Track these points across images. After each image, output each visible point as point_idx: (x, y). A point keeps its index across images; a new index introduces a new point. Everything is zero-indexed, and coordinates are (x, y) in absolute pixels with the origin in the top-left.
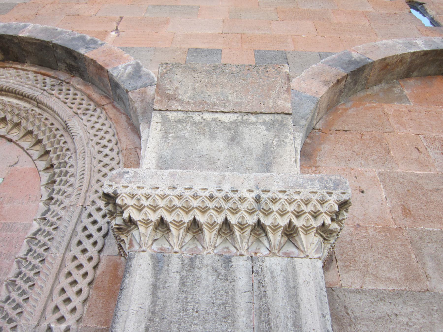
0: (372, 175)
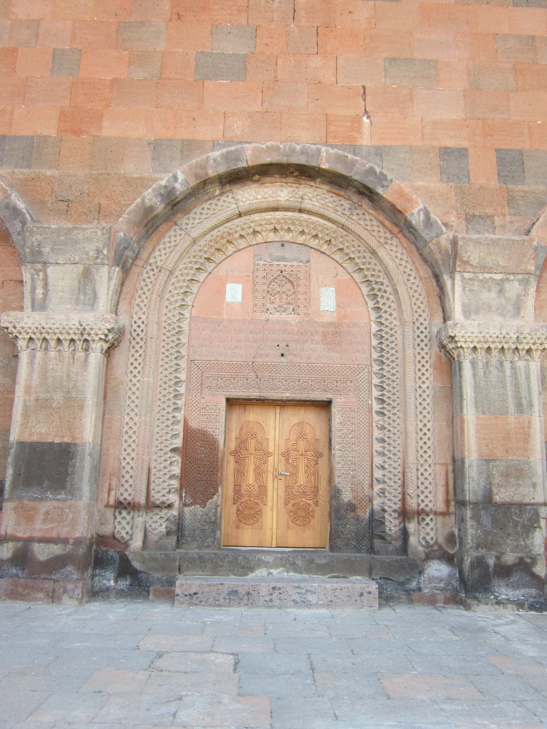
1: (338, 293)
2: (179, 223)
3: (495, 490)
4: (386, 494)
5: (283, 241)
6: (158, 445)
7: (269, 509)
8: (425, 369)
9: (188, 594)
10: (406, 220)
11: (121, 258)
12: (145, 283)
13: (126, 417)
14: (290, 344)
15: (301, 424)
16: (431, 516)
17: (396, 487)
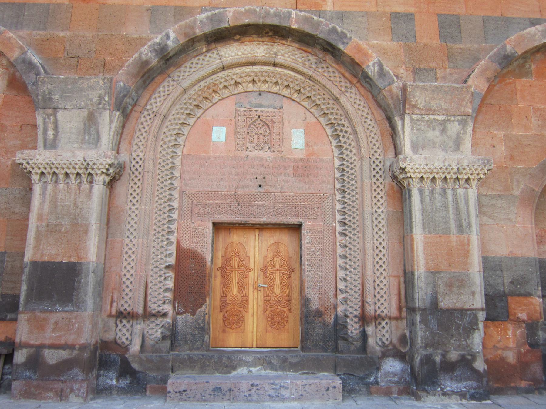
0: (500, 136)
1: (306, 134)
2: (171, 75)
3: (440, 298)
4: (348, 302)
5: (260, 91)
6: (154, 263)
7: (250, 315)
8: (380, 196)
9: (178, 391)
10: (363, 71)
11: (121, 104)
12: (143, 126)
13: (126, 240)
14: (266, 177)
15: (276, 243)
16: (387, 320)
17: (357, 296)
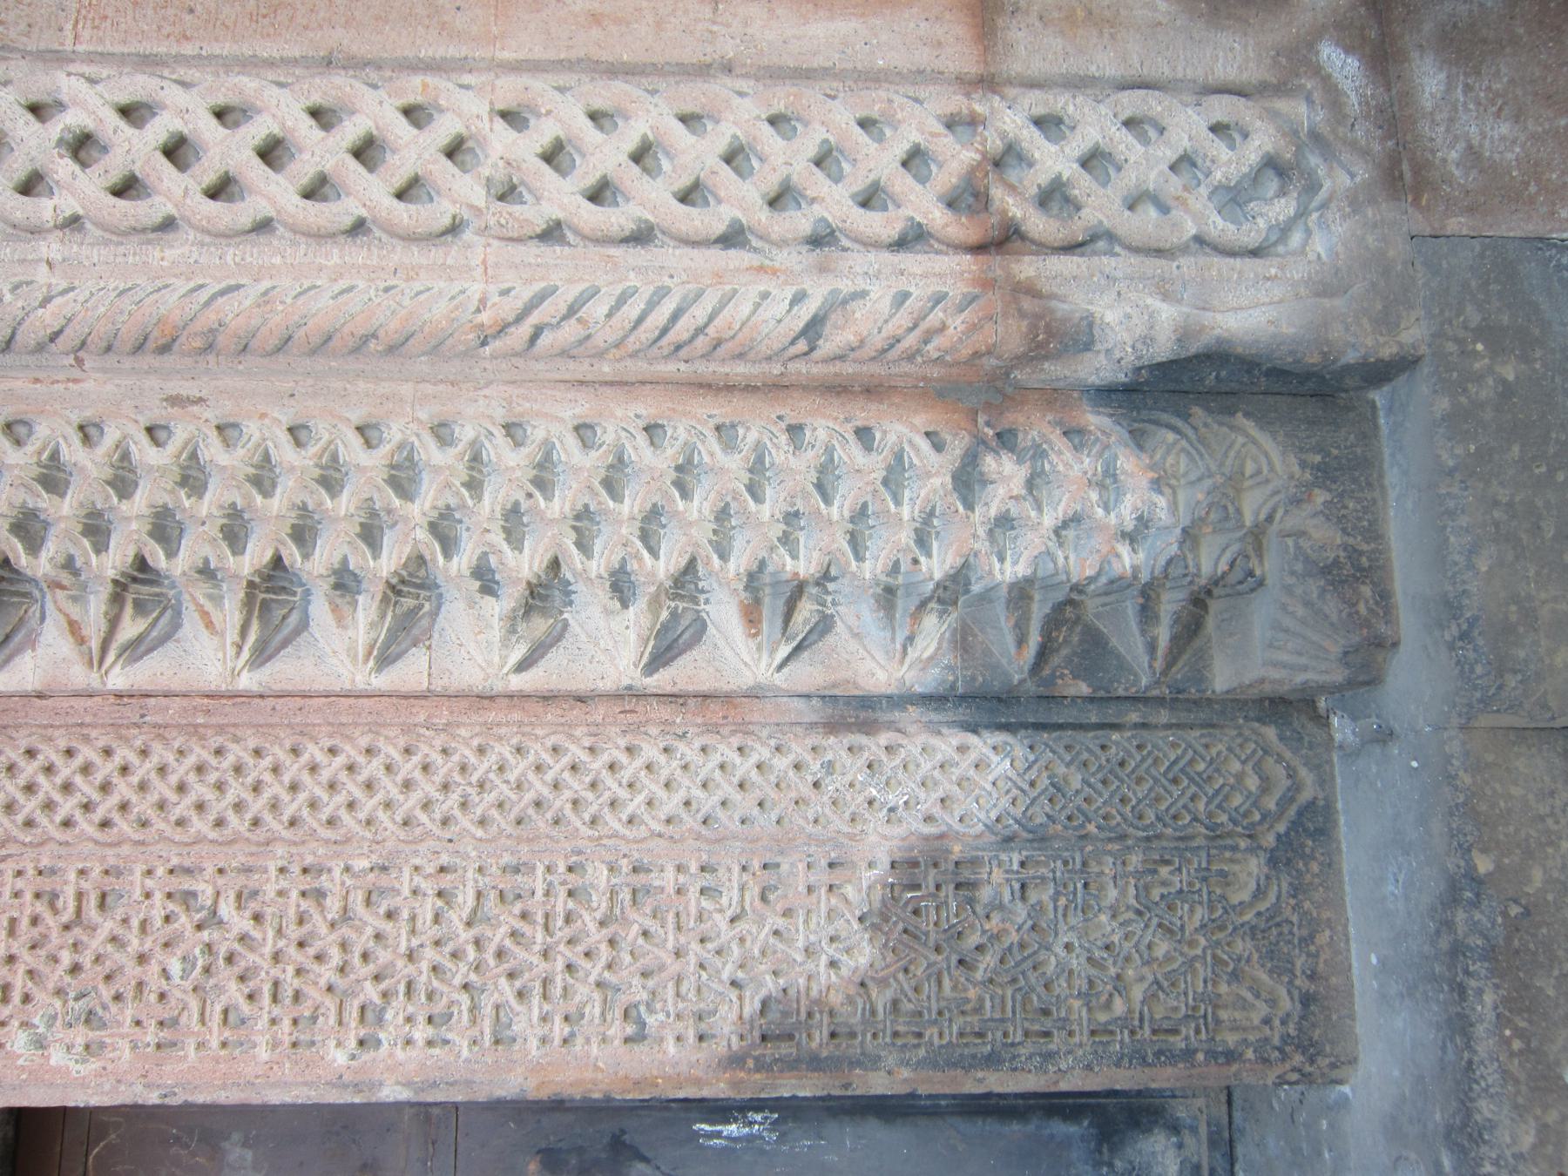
4: (805, 565)
17: (735, 465)
